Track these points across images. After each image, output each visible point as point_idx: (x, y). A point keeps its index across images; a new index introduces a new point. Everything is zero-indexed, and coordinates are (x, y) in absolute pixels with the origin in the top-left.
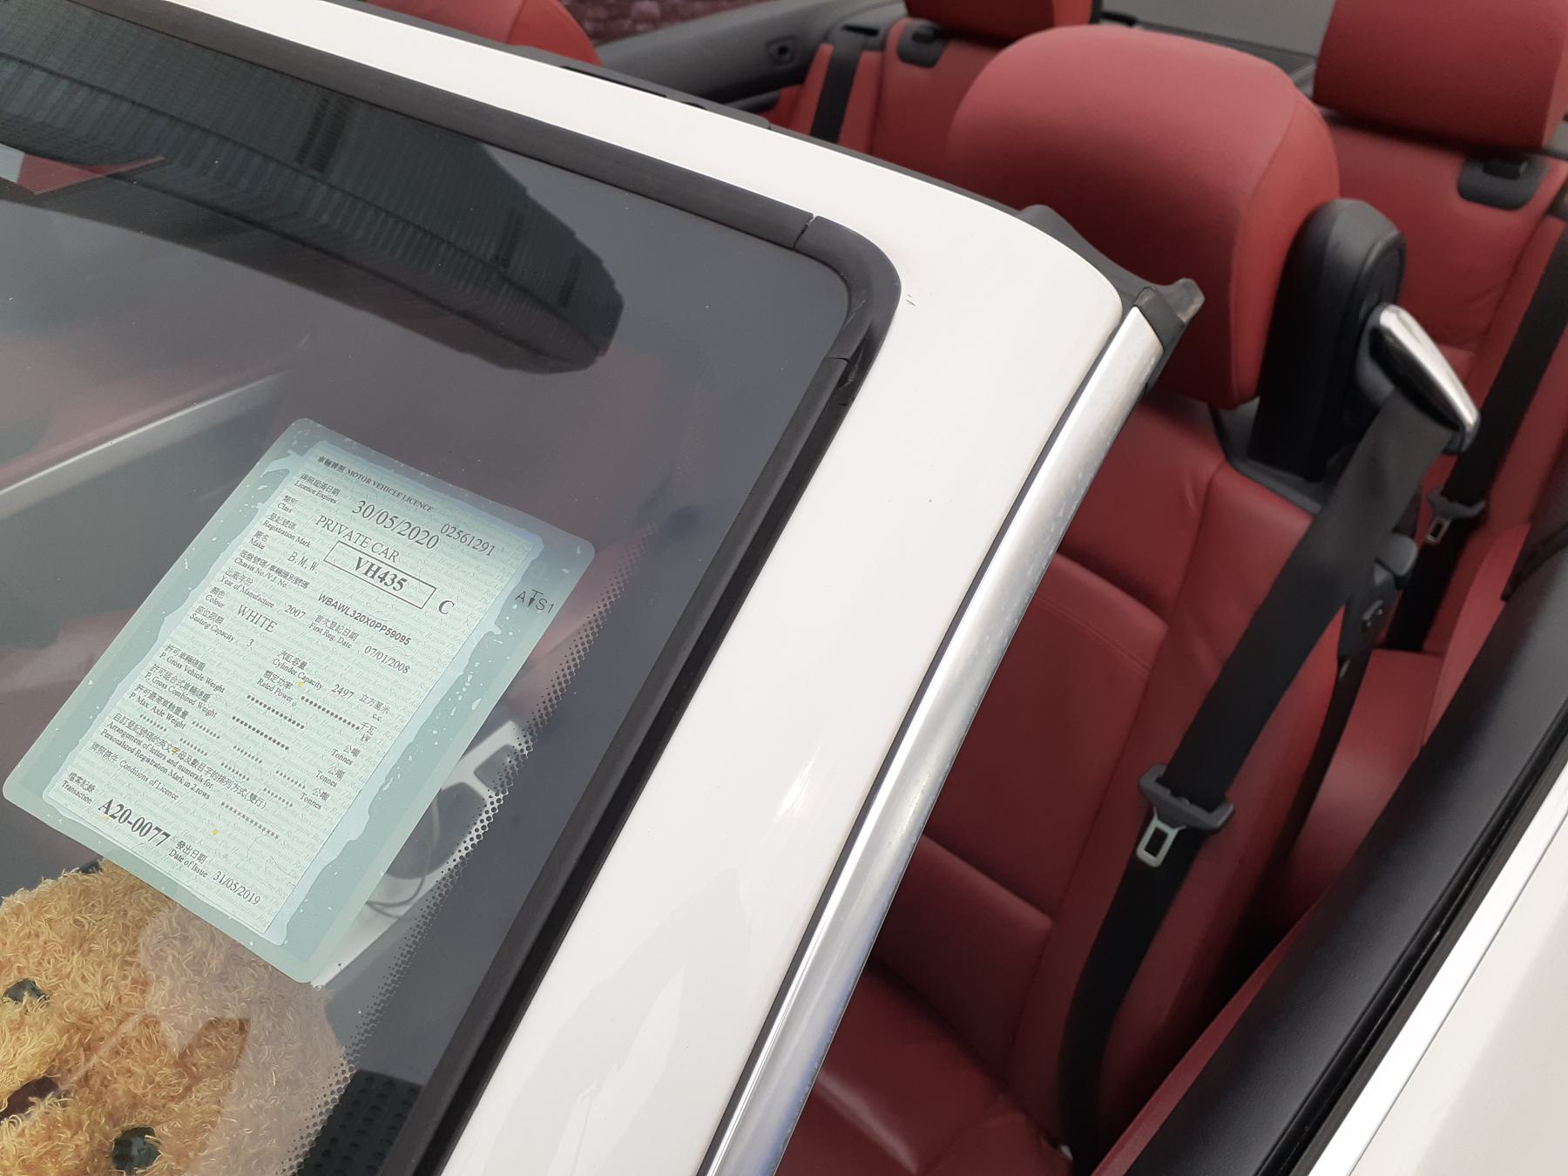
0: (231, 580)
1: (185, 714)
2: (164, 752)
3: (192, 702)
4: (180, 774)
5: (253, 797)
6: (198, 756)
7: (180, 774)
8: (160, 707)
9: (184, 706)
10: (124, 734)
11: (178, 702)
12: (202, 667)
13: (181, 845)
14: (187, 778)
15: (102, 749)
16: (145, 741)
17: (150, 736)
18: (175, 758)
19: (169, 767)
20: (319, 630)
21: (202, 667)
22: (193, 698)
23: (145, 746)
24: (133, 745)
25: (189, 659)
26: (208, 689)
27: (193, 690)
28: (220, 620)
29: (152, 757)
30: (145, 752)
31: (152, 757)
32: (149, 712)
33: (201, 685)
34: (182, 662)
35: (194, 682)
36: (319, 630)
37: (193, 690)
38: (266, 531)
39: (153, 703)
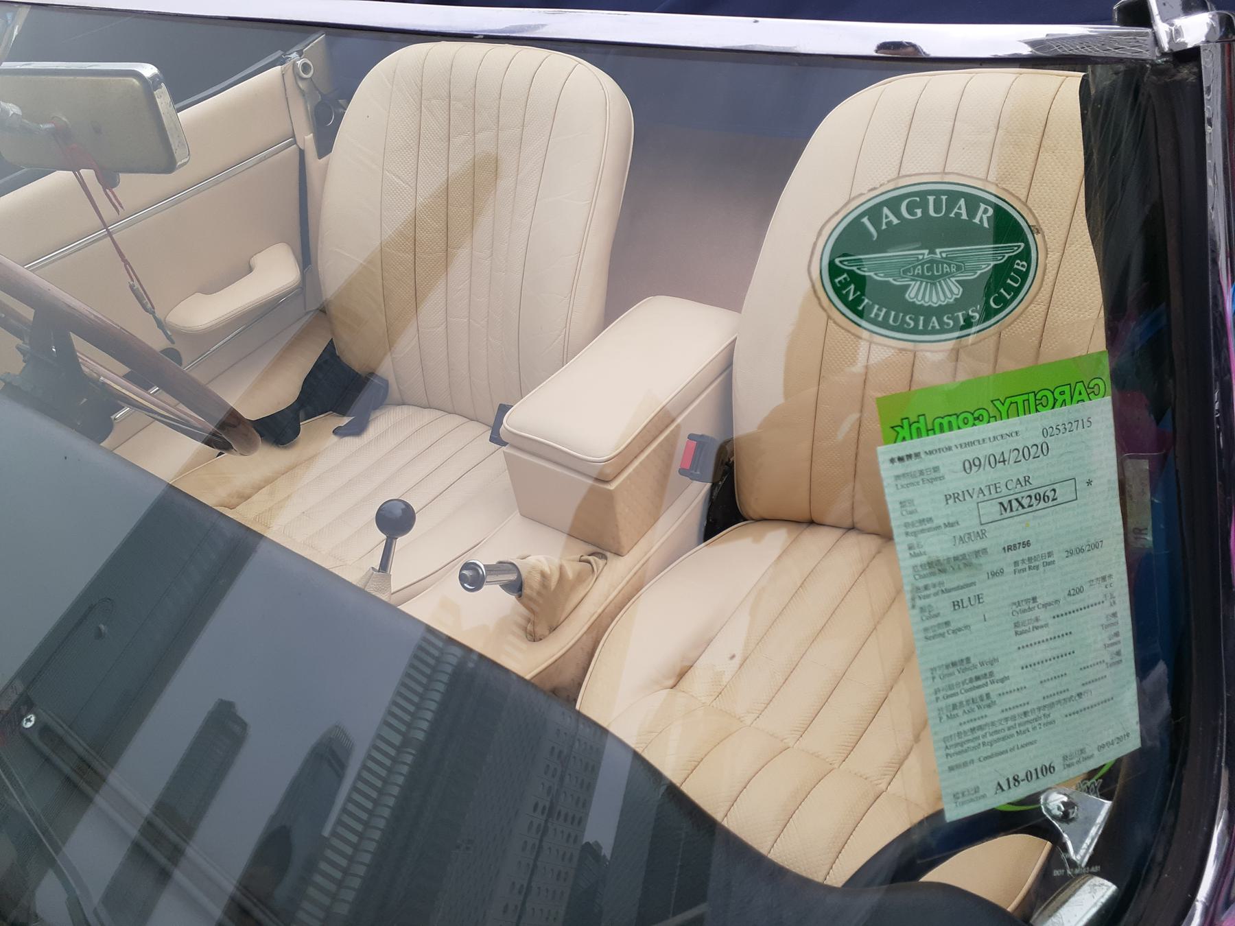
0: (927, 592)
1: (988, 695)
2: (1000, 727)
3: (986, 684)
4: (1022, 728)
5: (1080, 695)
6: (1020, 710)
7: (1022, 728)
8: (966, 708)
9: (983, 691)
10: (961, 744)
11: (974, 694)
12: (968, 659)
13: (1065, 758)
14: (1029, 726)
15: (958, 766)
16: (980, 733)
17: (980, 728)
18: (1010, 723)
19: (1013, 731)
20: (1024, 570)
21: (968, 659)
22: (979, 683)
23: (984, 736)
24: (976, 744)
25: (954, 664)
26: (986, 670)
27: (978, 678)
28: (947, 623)
29: (995, 737)
30: (989, 738)
31: (995, 737)
32: (966, 718)
33: (980, 671)
34: (951, 670)
35: (972, 674)
36: (1024, 570)
37: (978, 678)
38: (911, 539)
39: (960, 712)
